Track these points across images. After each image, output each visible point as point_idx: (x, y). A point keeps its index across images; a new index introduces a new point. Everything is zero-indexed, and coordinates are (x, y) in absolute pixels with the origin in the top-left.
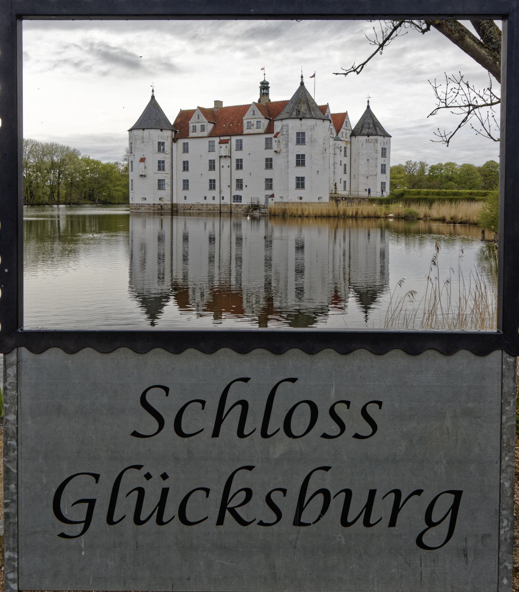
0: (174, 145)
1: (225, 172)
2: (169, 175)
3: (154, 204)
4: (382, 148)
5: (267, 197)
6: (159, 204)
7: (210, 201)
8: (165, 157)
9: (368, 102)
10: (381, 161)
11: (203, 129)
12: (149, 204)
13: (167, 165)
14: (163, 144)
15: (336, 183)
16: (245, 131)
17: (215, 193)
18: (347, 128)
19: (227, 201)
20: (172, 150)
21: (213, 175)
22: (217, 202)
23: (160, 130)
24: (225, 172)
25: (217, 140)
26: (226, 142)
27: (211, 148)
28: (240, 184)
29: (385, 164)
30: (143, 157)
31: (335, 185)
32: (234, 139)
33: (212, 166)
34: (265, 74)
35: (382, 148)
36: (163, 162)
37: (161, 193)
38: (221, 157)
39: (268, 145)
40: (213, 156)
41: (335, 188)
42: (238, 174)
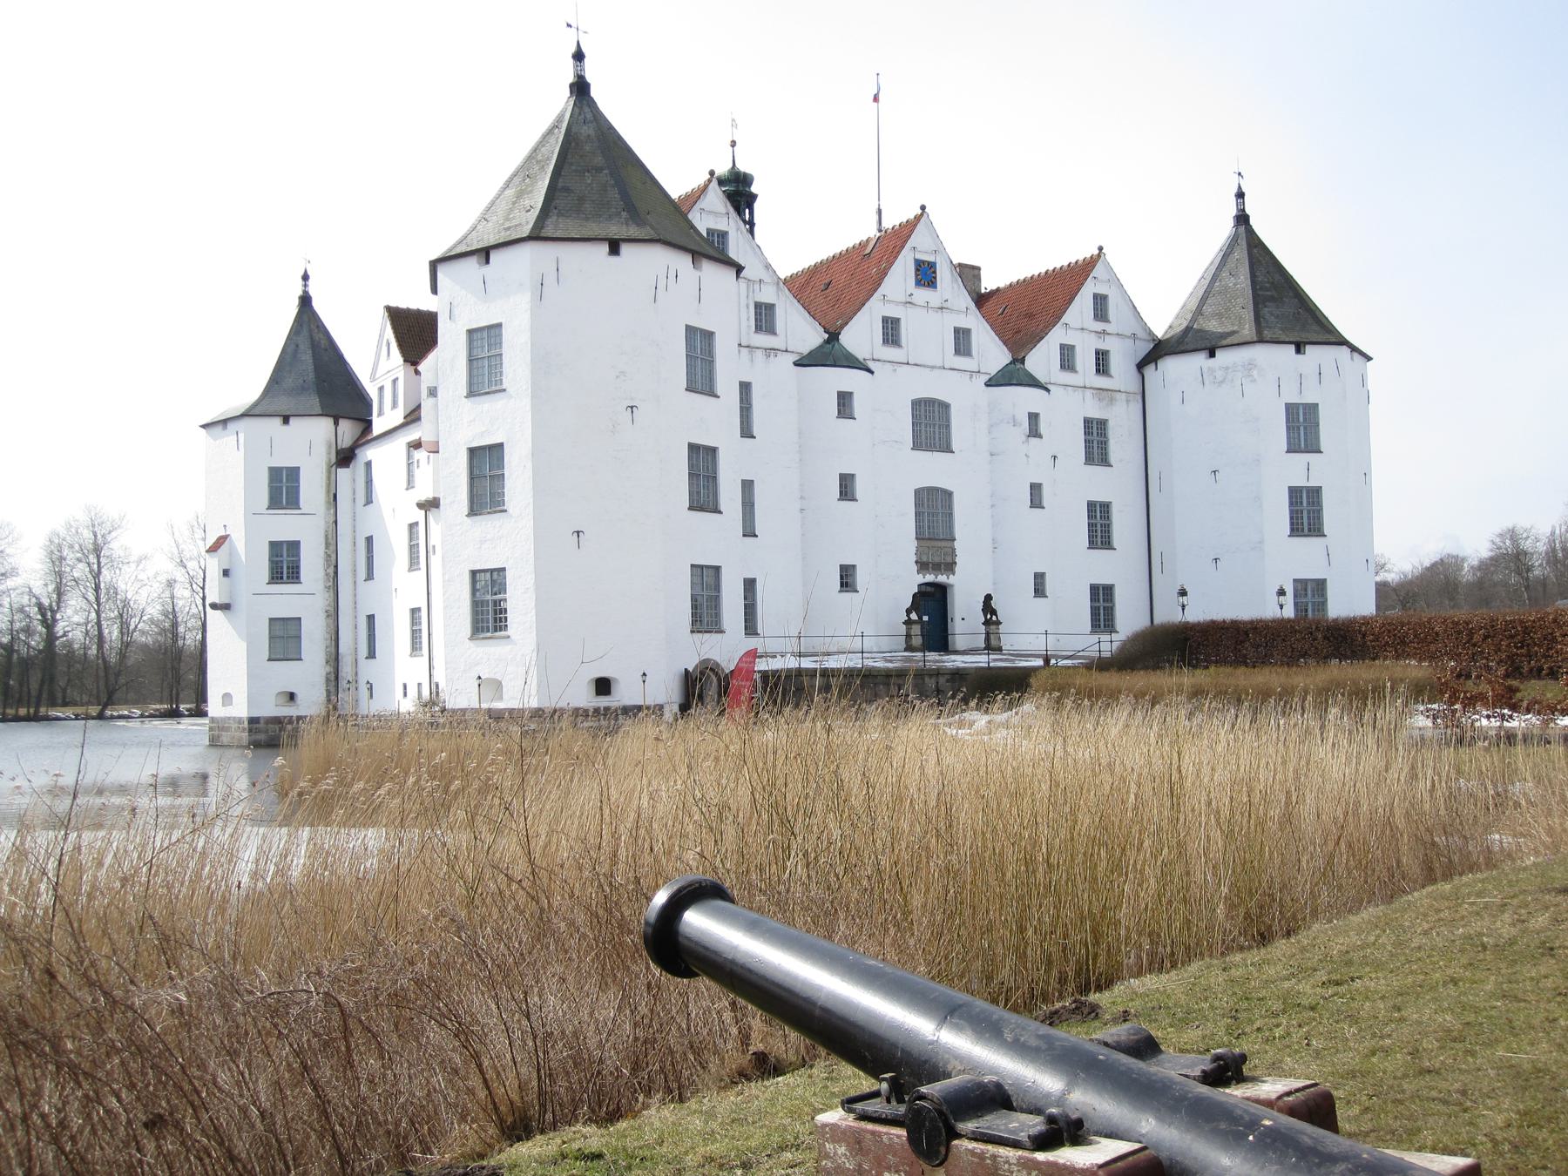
0: (343, 473)
2: (321, 601)
3: (253, 721)
4: (1291, 409)
6: (277, 721)
8: (304, 527)
9: (1240, 195)
10: (1297, 470)
12: (240, 720)
13: (311, 563)
14: (294, 473)
15: (988, 598)
18: (1109, 328)
20: (335, 496)
23: (278, 421)
29: (1312, 483)
30: (223, 534)
31: (988, 606)
34: (733, 144)
35: (1291, 409)
36: (294, 546)
37: (288, 675)
38: (420, 506)
41: (987, 623)
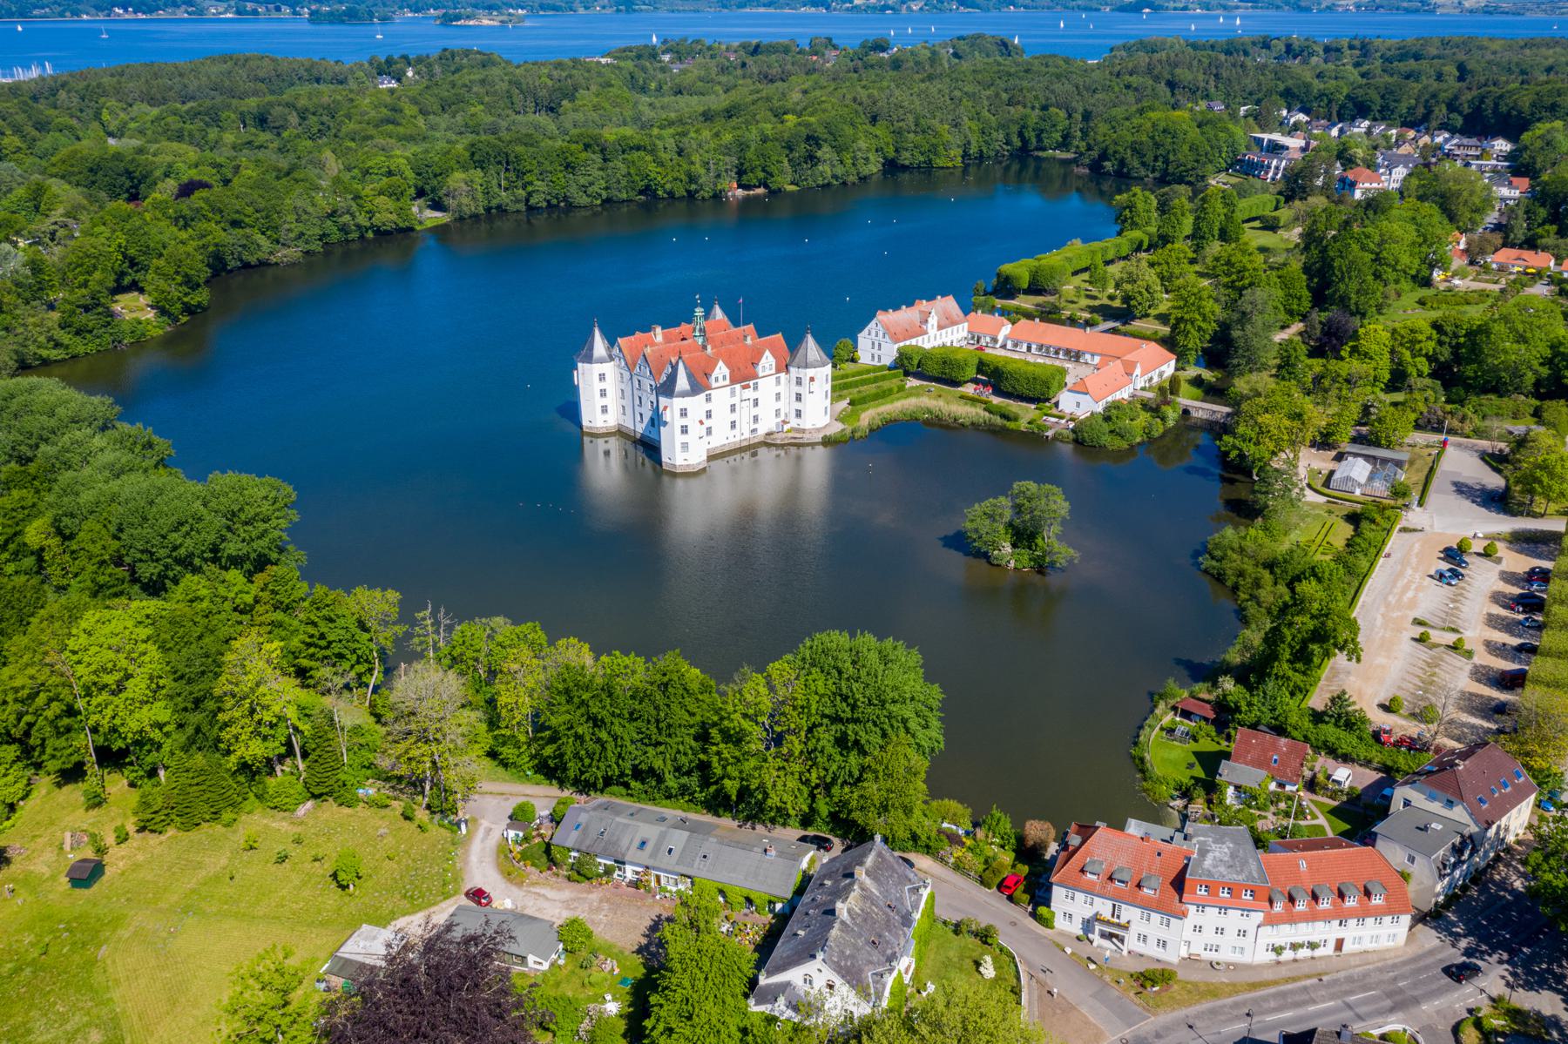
1: (745, 412)
5: (777, 424)
7: (732, 440)
11: (724, 378)
16: (761, 374)
17: (737, 431)
19: (747, 435)
21: (734, 417)
22: (738, 439)
24: (745, 412)
25: (738, 387)
26: (747, 387)
27: (733, 393)
28: (756, 419)
32: (751, 383)
33: (733, 408)
39: (778, 381)
40: (733, 401)
42: (755, 411)
